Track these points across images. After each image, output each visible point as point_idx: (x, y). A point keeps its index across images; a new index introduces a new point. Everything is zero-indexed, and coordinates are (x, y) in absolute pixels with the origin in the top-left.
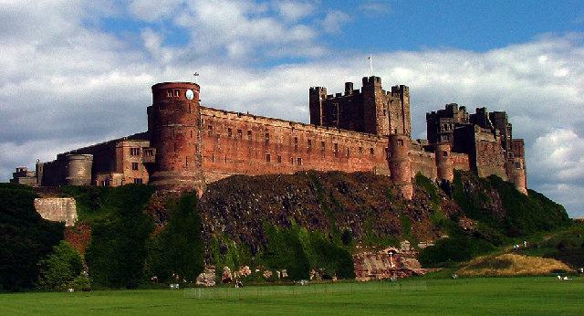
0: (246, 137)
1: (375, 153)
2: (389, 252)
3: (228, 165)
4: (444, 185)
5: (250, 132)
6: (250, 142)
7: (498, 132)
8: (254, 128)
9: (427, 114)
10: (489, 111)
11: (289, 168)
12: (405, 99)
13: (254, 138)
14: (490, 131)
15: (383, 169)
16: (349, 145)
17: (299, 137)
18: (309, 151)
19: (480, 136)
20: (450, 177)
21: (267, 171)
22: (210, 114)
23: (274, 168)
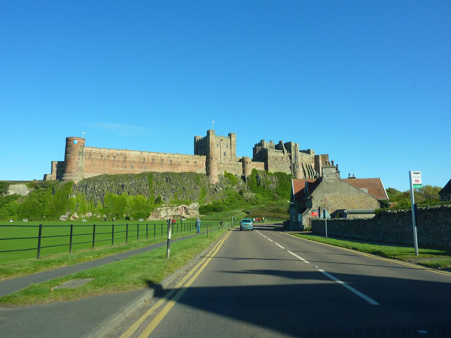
0: (112, 159)
1: (198, 163)
2: (182, 207)
3: (100, 170)
5: (114, 157)
6: (114, 161)
8: (117, 154)
10: (284, 142)
11: (138, 171)
13: (116, 159)
14: (282, 151)
17: (146, 158)
18: (152, 164)
19: (272, 154)
20: (249, 173)
21: (124, 173)
22: (91, 149)
23: (129, 171)
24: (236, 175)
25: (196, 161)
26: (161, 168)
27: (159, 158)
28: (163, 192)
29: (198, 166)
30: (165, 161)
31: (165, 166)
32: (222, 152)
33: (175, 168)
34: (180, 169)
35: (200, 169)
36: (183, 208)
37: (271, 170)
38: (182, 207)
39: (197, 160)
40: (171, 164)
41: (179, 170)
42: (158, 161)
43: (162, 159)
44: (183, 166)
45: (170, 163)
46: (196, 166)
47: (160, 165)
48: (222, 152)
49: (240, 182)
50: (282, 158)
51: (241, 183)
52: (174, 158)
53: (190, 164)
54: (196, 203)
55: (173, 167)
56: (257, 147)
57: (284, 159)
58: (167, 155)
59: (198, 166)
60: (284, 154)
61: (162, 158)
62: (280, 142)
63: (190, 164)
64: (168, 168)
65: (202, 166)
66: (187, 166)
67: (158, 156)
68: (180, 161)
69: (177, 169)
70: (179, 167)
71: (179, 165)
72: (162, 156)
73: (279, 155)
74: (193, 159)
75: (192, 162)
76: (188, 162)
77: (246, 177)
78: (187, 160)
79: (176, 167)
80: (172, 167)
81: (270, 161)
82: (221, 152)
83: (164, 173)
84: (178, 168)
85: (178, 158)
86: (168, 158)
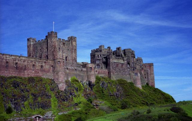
2: (36, 117)
4: (90, 84)
7: (125, 59)
9: (92, 51)
10: (123, 48)
12: (74, 43)
15: (49, 76)
16: (26, 63)
19: (113, 60)
20: (93, 80)
25: (42, 65)
26: (6, 72)
27: (4, 61)
28: (13, 100)
29: (44, 71)
30: (11, 64)
31: (11, 70)
32: (64, 57)
33: (21, 72)
34: (27, 73)
35: (46, 74)
36: (37, 118)
37: (114, 78)
38: (36, 117)
39: (44, 64)
43: (7, 62)
44: (30, 70)
45: (15, 66)
46: (41, 71)
47: (5, 69)
49: (87, 89)
50: (122, 64)
52: (20, 60)
53: (36, 68)
54: (50, 112)
56: (97, 54)
57: (124, 66)
58: (12, 57)
59: (44, 71)
60: (124, 60)
61: (7, 61)
62: (118, 49)
63: (36, 68)
64: (14, 73)
66: (33, 70)
67: (3, 58)
68: (26, 64)
69: (23, 73)
70: (26, 71)
71: (25, 69)
72: (7, 58)
73: (120, 62)
74: (39, 63)
75: (39, 66)
77: (92, 83)
79: (22, 71)
80: (18, 71)
81: (112, 67)
83: (11, 78)
84: (24, 72)
86: (13, 61)
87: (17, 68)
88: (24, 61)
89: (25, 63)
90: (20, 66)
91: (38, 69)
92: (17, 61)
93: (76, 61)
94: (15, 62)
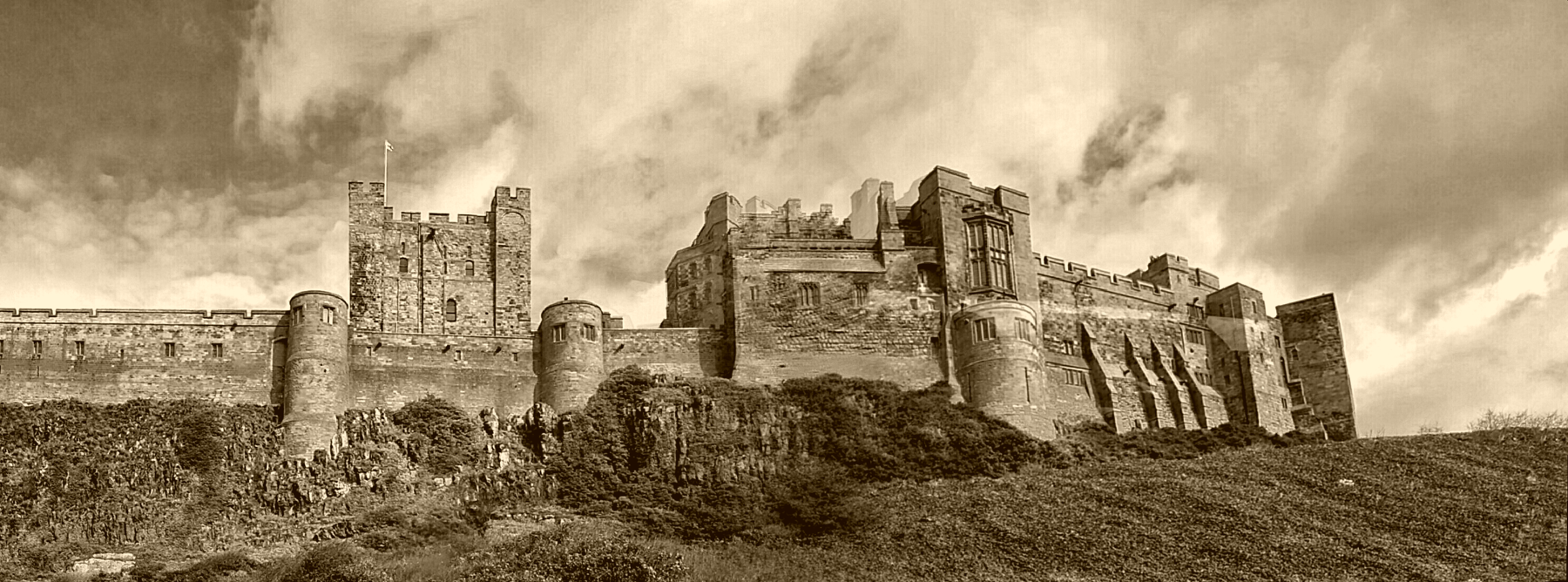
1: (230, 352)
16: (125, 340)
24: (483, 414)
26: (28, 384)
29: (230, 368)
33: (101, 381)
40: (87, 365)
41: (122, 392)
42: (19, 352)
48: (435, 299)
51: (504, 456)
53: (184, 359)
55: (88, 375)
59: (230, 368)
61: (37, 337)
65: (254, 370)
71: (121, 367)
75: (200, 346)
76: (170, 348)
78: (168, 337)
82: (427, 299)
85: (118, 330)
87: (78, 364)
88: (118, 330)
89: (123, 337)
90: (93, 357)
91: (189, 364)
92: (81, 336)
93: (520, 315)
94: (71, 339)
